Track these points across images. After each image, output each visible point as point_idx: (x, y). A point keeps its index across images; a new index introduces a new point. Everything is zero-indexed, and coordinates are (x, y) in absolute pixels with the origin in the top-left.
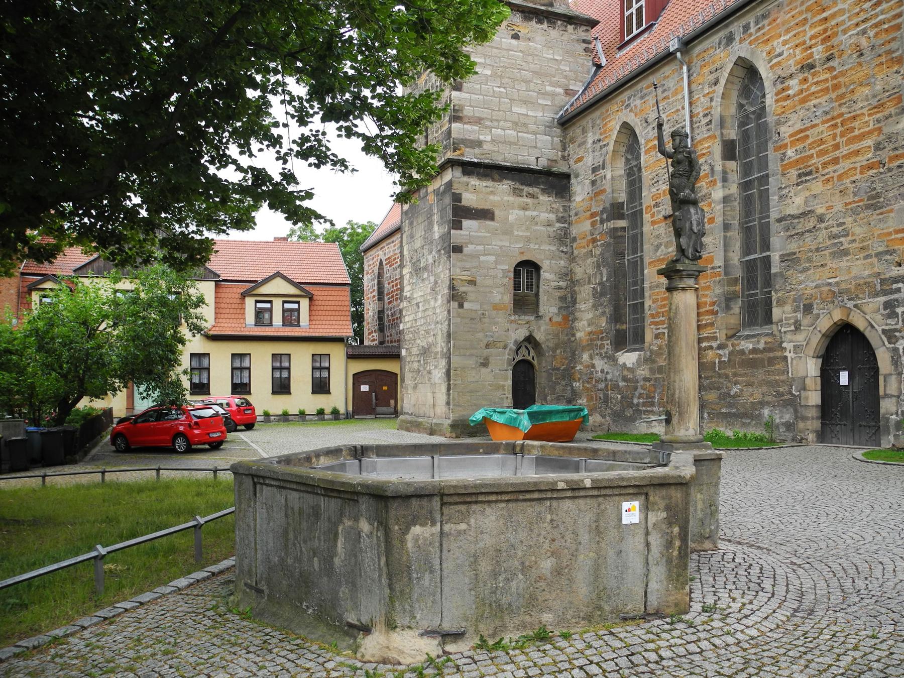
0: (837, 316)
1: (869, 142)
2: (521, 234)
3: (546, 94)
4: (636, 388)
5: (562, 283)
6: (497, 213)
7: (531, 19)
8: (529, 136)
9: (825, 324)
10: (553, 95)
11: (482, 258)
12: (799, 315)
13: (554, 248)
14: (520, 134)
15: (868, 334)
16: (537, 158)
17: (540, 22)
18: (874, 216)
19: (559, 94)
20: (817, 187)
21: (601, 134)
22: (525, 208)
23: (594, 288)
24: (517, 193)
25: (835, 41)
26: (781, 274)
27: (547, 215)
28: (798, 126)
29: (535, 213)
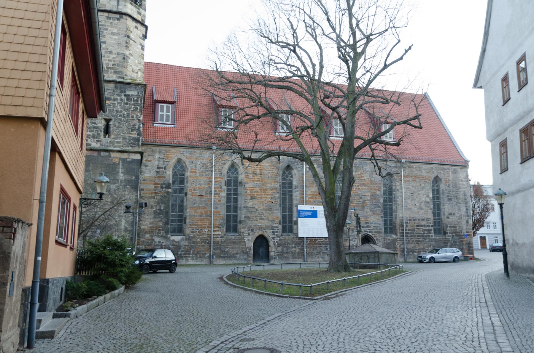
0: (260, 233)
1: (270, 196)
4: (180, 249)
9: (257, 235)
12: (250, 231)
15: (268, 238)
18: (271, 213)
20: (256, 202)
25: (263, 171)
26: (245, 221)
28: (251, 186)
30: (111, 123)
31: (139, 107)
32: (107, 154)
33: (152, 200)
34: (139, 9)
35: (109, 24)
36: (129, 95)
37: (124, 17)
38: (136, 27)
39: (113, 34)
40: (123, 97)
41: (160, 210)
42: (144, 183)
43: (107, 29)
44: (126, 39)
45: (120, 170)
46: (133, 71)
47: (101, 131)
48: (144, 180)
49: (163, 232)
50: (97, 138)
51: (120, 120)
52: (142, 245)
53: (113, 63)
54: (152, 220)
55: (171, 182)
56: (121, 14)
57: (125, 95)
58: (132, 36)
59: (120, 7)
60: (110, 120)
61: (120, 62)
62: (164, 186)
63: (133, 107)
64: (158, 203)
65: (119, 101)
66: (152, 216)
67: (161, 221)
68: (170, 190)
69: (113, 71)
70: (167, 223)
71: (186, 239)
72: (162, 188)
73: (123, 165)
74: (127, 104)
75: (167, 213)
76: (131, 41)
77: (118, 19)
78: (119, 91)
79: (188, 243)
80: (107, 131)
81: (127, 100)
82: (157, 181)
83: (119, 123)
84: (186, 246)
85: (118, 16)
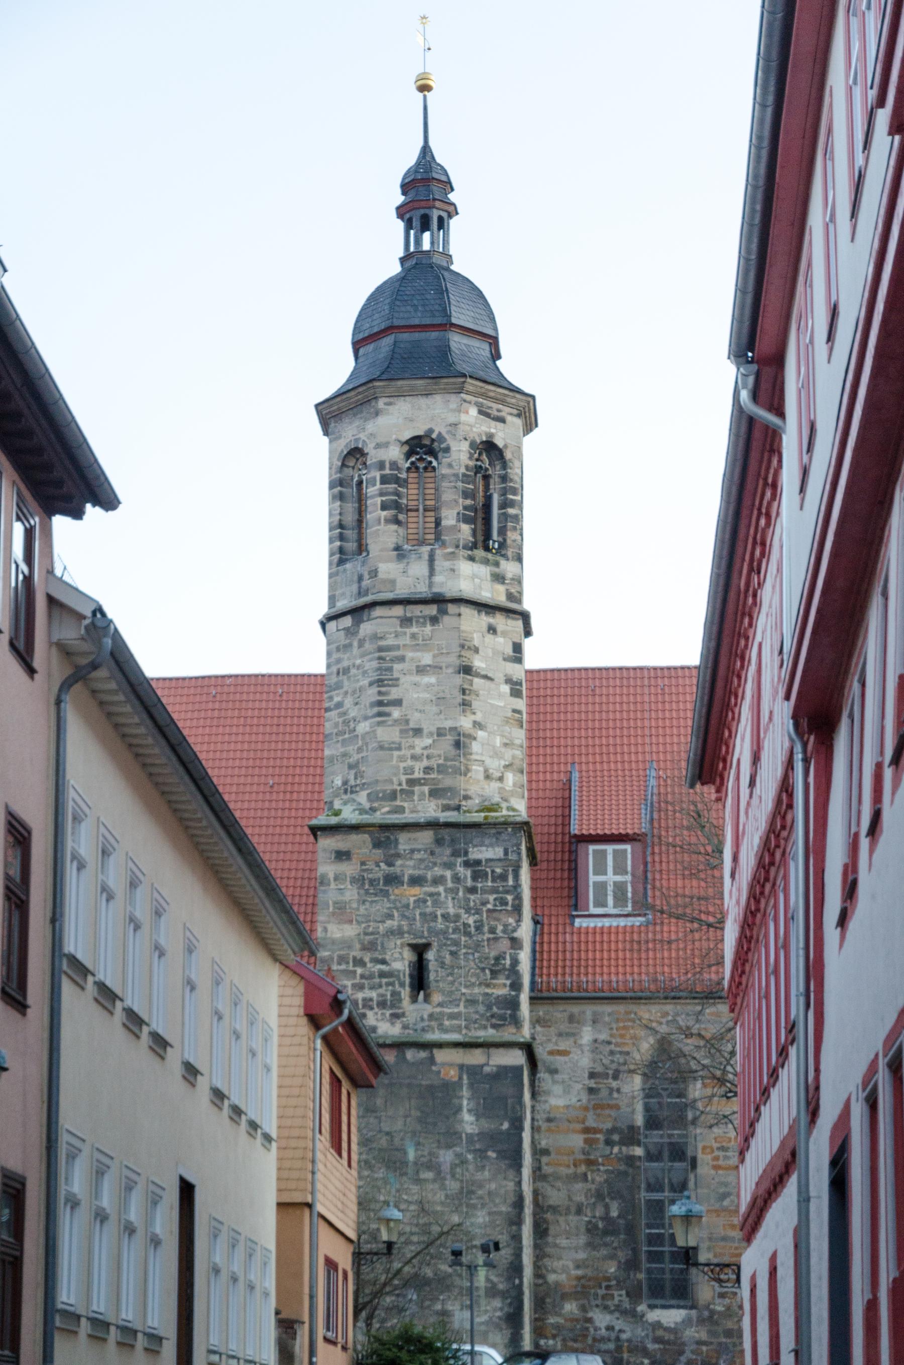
4: (681, 1353)
21: (612, 1036)
23: (590, 1222)
30: (430, 955)
31: (510, 898)
32: (423, 1054)
33: (579, 1186)
34: (497, 564)
35: (407, 640)
36: (478, 862)
37: (452, 608)
38: (492, 630)
39: (421, 670)
40: (460, 869)
41: (606, 1218)
42: (549, 1130)
43: (402, 659)
44: (459, 679)
45: (465, 1102)
46: (488, 777)
47: (402, 985)
48: (549, 1120)
49: (620, 1296)
50: (393, 1006)
51: (456, 943)
52: (554, 1337)
53: (425, 763)
54: (582, 1255)
55: (639, 1120)
56: (440, 601)
57: (467, 864)
58: (478, 663)
59: (438, 579)
60: (427, 946)
61: (446, 759)
62: (616, 1137)
63: (491, 898)
64: (599, 1196)
65: (450, 885)
66: (582, 1240)
67: (612, 1257)
68: (639, 1151)
69: (426, 789)
70: (632, 1264)
71: (701, 1321)
72: (609, 1143)
73: (471, 1086)
74: (473, 890)
75: (631, 1230)
76: (476, 680)
77: (434, 620)
78: (448, 852)
79: (710, 1332)
80: (419, 981)
81: (475, 878)
82: (591, 1122)
83: (453, 953)
84: (700, 1343)
85: (432, 610)
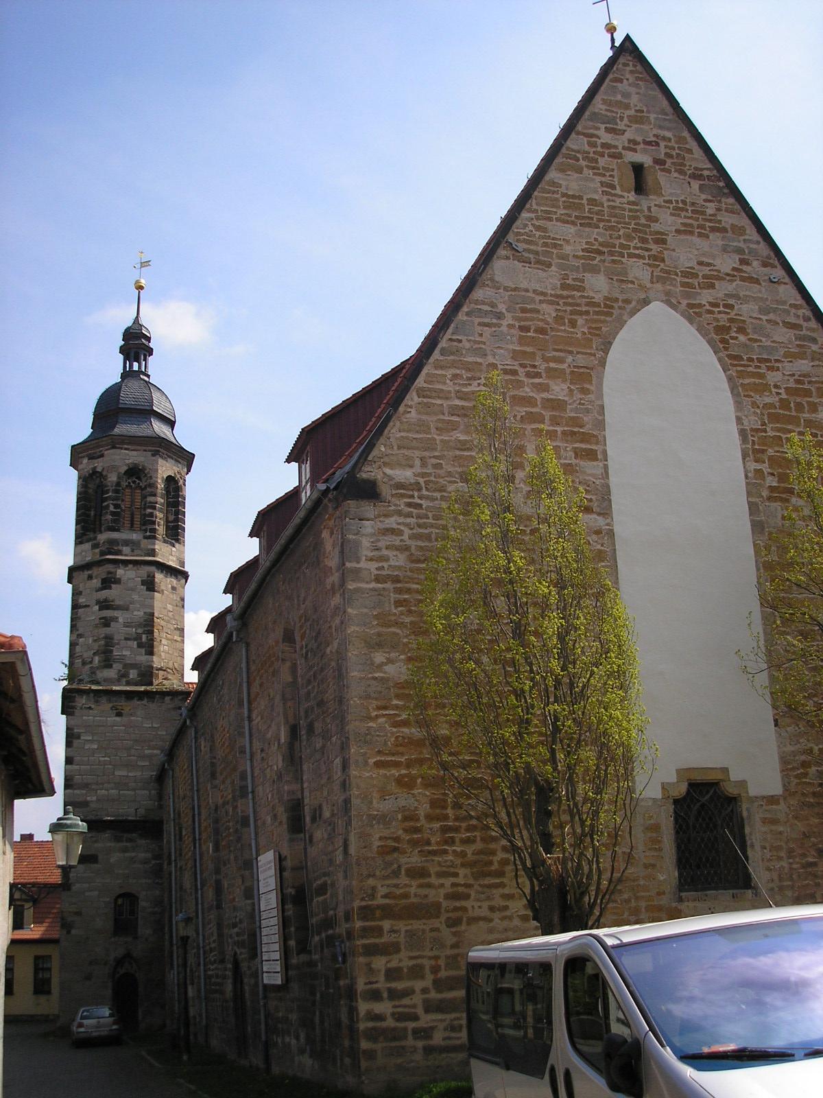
2: (121, 872)
3: (143, 757)
5: (156, 909)
6: (100, 857)
7: (132, 698)
8: (129, 792)
10: (150, 757)
11: (87, 894)
13: (150, 881)
14: (121, 792)
16: (136, 810)
17: (140, 699)
19: (157, 755)
22: (125, 850)
24: (118, 839)
27: (143, 855)
29: (133, 854)
